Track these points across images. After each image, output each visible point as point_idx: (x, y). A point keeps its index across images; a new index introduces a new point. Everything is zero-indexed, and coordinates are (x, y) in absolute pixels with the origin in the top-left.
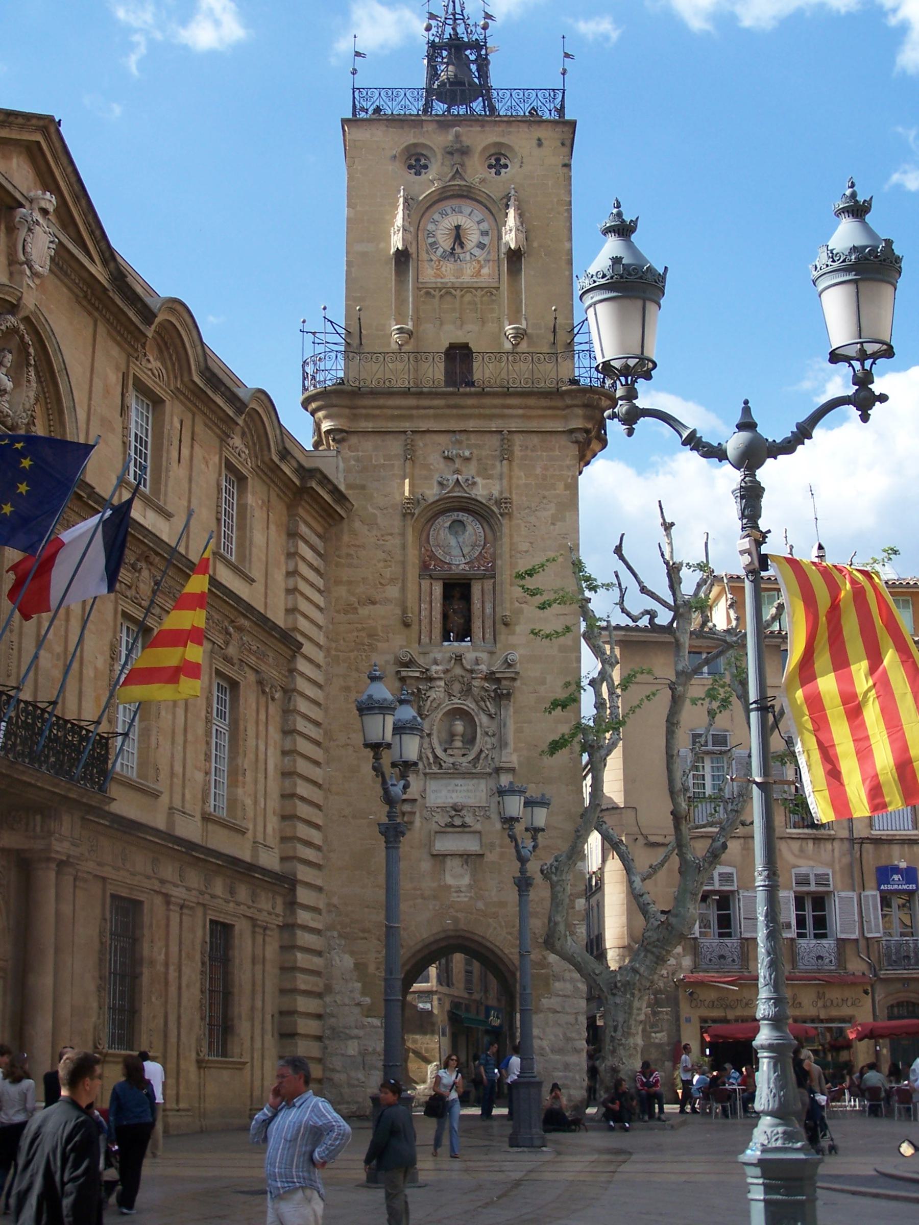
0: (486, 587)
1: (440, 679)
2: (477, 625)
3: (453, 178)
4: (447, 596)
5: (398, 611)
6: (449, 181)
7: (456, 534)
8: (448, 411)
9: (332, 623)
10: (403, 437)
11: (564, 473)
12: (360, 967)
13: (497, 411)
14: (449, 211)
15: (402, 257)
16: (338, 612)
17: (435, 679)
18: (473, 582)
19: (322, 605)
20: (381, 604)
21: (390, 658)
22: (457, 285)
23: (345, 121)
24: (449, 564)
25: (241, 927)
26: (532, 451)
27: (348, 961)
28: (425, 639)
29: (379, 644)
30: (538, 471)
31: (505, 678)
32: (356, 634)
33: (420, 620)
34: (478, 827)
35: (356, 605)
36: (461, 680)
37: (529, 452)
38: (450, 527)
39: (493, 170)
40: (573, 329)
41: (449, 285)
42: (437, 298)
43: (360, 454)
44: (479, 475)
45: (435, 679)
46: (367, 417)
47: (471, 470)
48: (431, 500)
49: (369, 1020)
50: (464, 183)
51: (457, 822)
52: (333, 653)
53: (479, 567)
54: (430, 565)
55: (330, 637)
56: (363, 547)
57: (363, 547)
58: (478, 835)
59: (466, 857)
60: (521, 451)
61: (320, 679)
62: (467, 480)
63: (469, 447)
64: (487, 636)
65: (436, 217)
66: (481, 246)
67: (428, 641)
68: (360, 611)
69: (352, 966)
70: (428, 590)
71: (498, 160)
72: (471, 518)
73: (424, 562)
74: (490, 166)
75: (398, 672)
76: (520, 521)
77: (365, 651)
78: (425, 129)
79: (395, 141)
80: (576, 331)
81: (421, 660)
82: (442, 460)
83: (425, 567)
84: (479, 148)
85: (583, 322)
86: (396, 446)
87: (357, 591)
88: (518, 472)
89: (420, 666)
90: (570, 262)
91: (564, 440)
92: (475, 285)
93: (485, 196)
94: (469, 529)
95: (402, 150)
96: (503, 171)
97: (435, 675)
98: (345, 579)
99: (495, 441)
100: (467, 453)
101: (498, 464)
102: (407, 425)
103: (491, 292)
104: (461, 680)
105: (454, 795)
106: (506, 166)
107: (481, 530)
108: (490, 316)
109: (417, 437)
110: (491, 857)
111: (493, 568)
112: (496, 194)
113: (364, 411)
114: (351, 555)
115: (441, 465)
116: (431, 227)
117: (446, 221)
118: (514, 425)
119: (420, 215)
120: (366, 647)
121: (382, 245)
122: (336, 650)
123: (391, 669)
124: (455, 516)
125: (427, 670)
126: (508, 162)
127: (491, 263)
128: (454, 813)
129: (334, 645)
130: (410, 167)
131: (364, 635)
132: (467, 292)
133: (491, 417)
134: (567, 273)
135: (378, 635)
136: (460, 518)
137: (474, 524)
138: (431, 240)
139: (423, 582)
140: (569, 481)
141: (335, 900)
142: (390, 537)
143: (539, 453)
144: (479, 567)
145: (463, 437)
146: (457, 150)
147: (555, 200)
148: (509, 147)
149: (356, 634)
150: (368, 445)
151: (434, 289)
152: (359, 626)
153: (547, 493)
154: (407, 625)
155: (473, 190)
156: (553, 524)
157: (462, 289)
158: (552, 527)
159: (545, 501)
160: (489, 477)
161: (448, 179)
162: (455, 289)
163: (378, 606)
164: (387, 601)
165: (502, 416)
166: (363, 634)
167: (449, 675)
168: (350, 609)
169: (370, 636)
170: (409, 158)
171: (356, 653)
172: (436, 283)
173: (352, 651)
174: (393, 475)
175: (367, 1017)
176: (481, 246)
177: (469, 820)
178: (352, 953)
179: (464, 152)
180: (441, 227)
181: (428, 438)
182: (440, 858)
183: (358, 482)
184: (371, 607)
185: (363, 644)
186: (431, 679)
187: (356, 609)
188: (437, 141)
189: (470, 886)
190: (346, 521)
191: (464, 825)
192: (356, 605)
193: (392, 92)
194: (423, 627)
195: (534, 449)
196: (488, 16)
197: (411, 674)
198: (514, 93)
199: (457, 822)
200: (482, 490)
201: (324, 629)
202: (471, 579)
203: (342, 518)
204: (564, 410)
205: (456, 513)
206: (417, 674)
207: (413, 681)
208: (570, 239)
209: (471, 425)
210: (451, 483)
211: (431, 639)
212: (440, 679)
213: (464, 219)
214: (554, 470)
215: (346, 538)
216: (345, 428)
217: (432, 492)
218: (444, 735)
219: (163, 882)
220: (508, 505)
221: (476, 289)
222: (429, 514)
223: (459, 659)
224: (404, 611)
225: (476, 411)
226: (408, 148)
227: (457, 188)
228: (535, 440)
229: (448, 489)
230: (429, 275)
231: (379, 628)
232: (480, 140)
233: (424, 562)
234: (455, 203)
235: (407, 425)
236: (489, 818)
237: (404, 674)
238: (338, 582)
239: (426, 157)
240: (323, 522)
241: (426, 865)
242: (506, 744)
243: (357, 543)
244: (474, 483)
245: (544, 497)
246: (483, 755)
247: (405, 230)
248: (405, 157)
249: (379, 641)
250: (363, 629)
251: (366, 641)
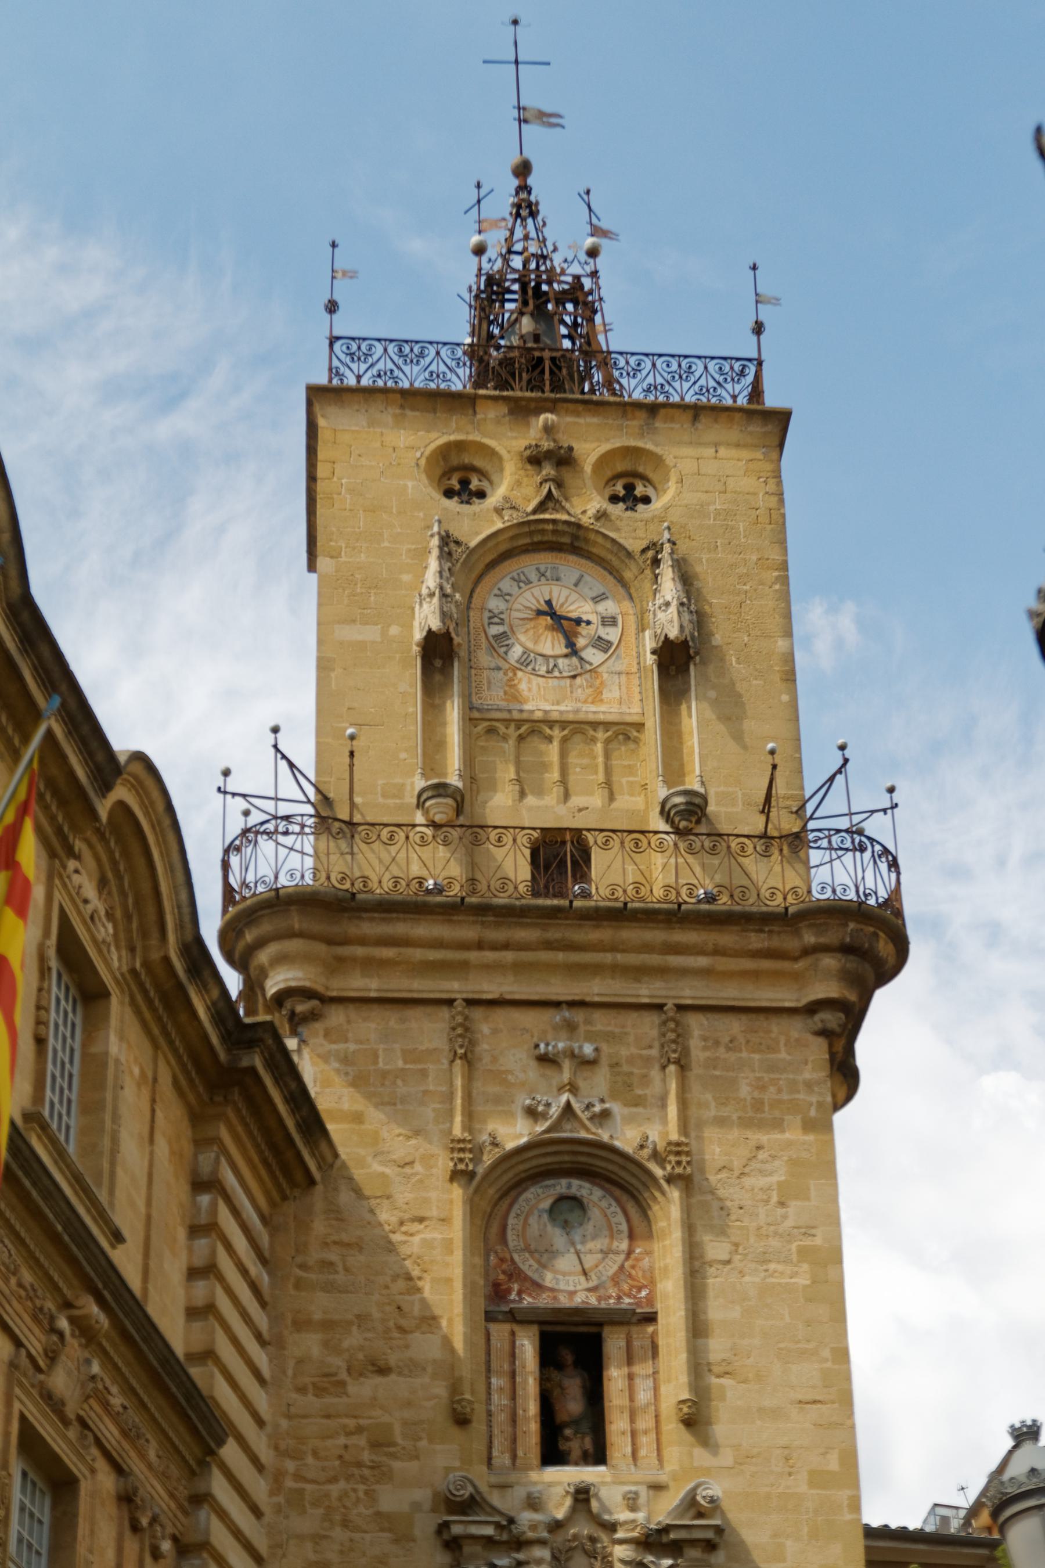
0: (636, 1343)
1: (542, 1542)
2: (617, 1426)
3: (541, 507)
4: (548, 1358)
5: (441, 1390)
6: (535, 512)
7: (566, 1226)
8: (545, 956)
9: (289, 1417)
10: (445, 1013)
11: (801, 1096)
13: (654, 959)
14: (533, 576)
15: (438, 652)
16: (302, 1390)
17: (530, 1543)
18: (607, 1331)
19: (266, 1372)
20: (400, 1374)
21: (422, 1495)
22: (555, 716)
23: (315, 394)
24: (552, 1290)
26: (729, 1049)
28: (501, 1458)
29: (397, 1465)
30: (745, 1091)
31: (693, 1543)
32: (342, 1440)
33: (489, 1414)
35: (343, 1375)
36: (588, 1545)
37: (721, 1052)
38: (552, 1211)
39: (621, 506)
40: (803, 807)
41: (538, 715)
42: (512, 742)
43: (352, 1047)
44: (614, 1095)
45: (530, 1543)
46: (369, 965)
47: (597, 1085)
48: (510, 1145)
50: (565, 517)
52: (289, 1483)
53: (619, 1298)
54: (509, 1291)
55: (283, 1446)
56: (358, 1246)
57: (358, 1246)
60: (705, 1048)
61: (262, 1545)
62: (589, 1106)
63: (590, 1037)
64: (642, 1452)
65: (506, 585)
67: (507, 1460)
68: (351, 1389)
70: (507, 1347)
71: (630, 488)
72: (598, 1193)
73: (496, 1285)
74: (614, 499)
75: (445, 1526)
76: (709, 1197)
77: (364, 1480)
78: (479, 417)
79: (418, 440)
81: (495, 1499)
82: (533, 1063)
83: (497, 1293)
84: (592, 458)
86: (431, 1031)
87: (346, 1344)
88: (697, 1092)
89: (496, 1511)
91: (796, 1028)
92: (591, 717)
93: (609, 545)
94: (595, 1213)
95: (434, 452)
96: (641, 507)
97: (530, 1535)
98: (317, 1316)
99: (648, 1026)
100: (588, 1049)
101: (655, 1073)
102: (456, 985)
103: (624, 732)
104: (588, 1545)
107: (620, 1218)
108: (624, 780)
109: (477, 1013)
111: (650, 1300)
112: (634, 545)
113: (360, 951)
114: (331, 1264)
115: (533, 1072)
116: (495, 604)
117: (528, 594)
118: (690, 992)
119: (474, 575)
120: (367, 1472)
121: (394, 630)
122: (298, 1477)
123: (425, 1525)
124: (563, 1186)
125: (511, 1521)
126: (650, 492)
127: (623, 677)
129: (290, 1466)
130: (449, 493)
131: (361, 1441)
132: (574, 732)
133: (639, 972)
134: (785, 698)
135: (393, 1444)
136: (574, 1191)
137: (604, 1204)
138: (494, 630)
139: (494, 1328)
140: (813, 1113)
142: (416, 1227)
143: (744, 1055)
144: (619, 1298)
145: (579, 1016)
146: (549, 455)
147: (754, 558)
148: (657, 460)
149: (342, 1440)
150: (368, 1027)
151: (507, 722)
152: (351, 1423)
153: (764, 1138)
154: (462, 1421)
155: (581, 533)
156: (782, 1204)
157: (563, 724)
158: (780, 1211)
159: (762, 1155)
160: (638, 1102)
161: (530, 509)
162: (551, 724)
163: (393, 1377)
164: (413, 1368)
165: (662, 972)
166: (361, 1441)
167: (559, 1538)
168: (329, 1384)
169: (375, 1445)
170: (447, 474)
171: (342, 1484)
172: (509, 711)
173: (334, 1480)
174: (425, 1092)
179: (563, 459)
180: (516, 606)
181: (501, 1017)
183: (346, 1106)
184: (379, 1380)
185: (359, 1465)
186: (519, 1544)
187: (342, 1384)
188: (507, 441)
190: (319, 1188)
192: (343, 1375)
193: (409, 349)
194: (496, 1431)
195: (732, 1045)
196: (596, 231)
197: (474, 1530)
198: (660, 362)
201: (269, 1429)
202: (601, 1325)
203: (312, 1182)
204: (796, 959)
205: (564, 1182)
206: (489, 1531)
207: (478, 1549)
209: (596, 989)
210: (555, 1111)
211: (514, 1457)
212: (542, 1542)
213: (565, 592)
214: (780, 1091)
215: (319, 1226)
216: (320, 989)
217: (515, 1133)
220: (684, 1159)
221: (595, 725)
222: (505, 1178)
223: (582, 1495)
224: (455, 1388)
225: (608, 958)
226: (446, 451)
227: (550, 527)
228: (735, 1025)
229: (547, 1124)
230: (493, 697)
231: (397, 1429)
232: (592, 442)
233: (496, 1285)
234: (545, 560)
235: (455, 987)
237: (457, 1530)
238: (301, 1324)
239: (483, 474)
240: (270, 1184)
243: (344, 1237)
244: (605, 1114)
245: (758, 1148)
247: (444, 596)
248: (439, 472)
249: (394, 1456)
250: (359, 1430)
251: (366, 1456)
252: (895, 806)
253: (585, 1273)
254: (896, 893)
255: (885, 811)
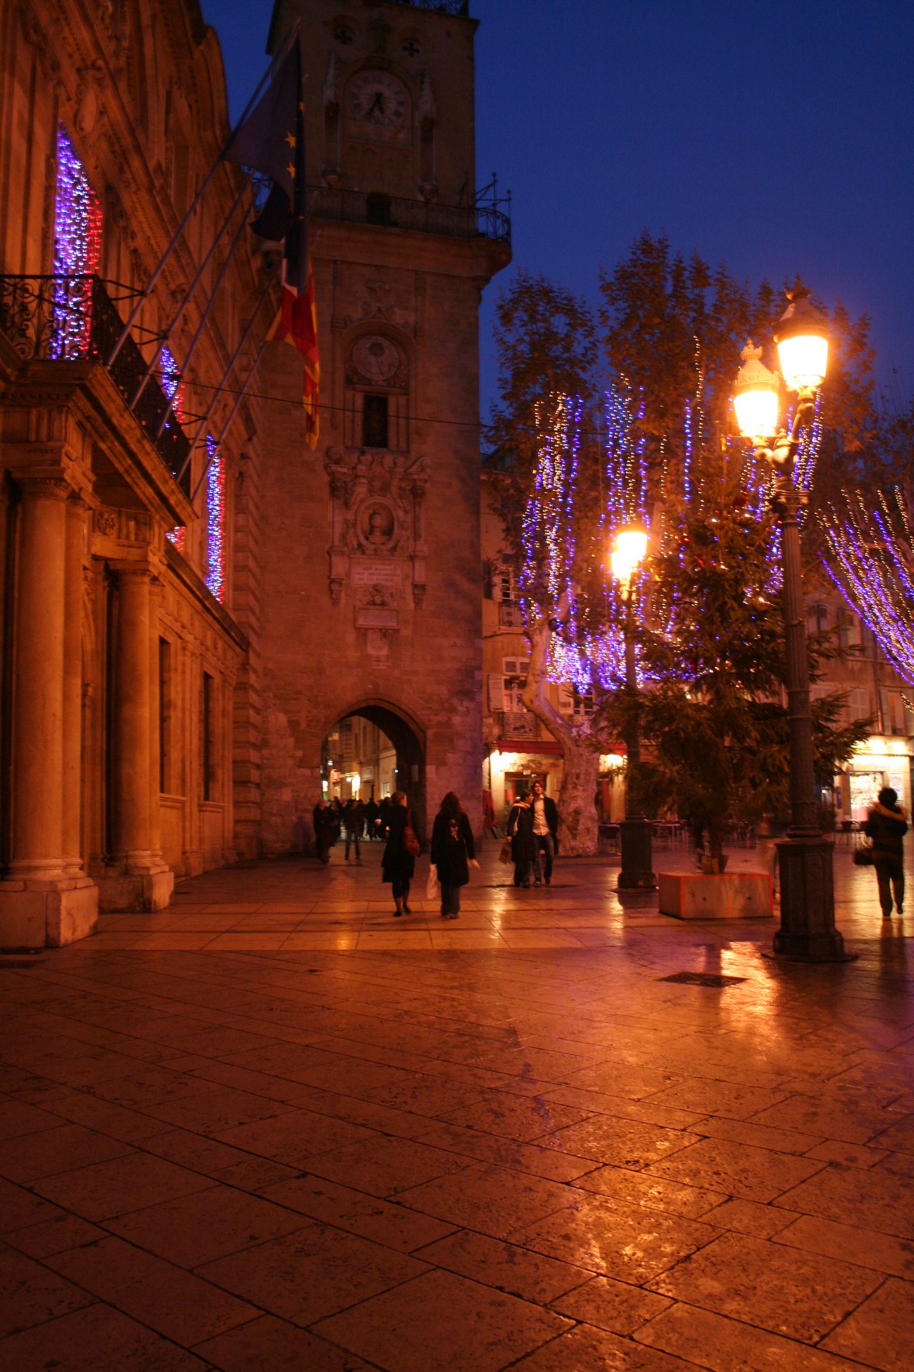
7: (375, 355)
12: (293, 724)
17: (360, 476)
24: (369, 379)
25: (217, 680)
27: (283, 718)
34: (394, 605)
49: (301, 770)
51: (378, 599)
58: (395, 613)
59: (385, 633)
66: (397, 114)
67: (350, 443)
69: (286, 723)
74: (405, 49)
80: (478, 196)
85: (489, 187)
90: (472, 139)
100: (387, 287)
105: (375, 577)
106: (418, 51)
110: (406, 632)
128: (375, 593)
141: (270, 665)
175: (300, 767)
176: (397, 114)
177: (387, 599)
178: (286, 712)
182: (362, 633)
189: (388, 657)
191: (383, 604)
199: (378, 599)
200: (400, 317)
205: (374, 337)
208: (473, 119)
212: (364, 477)
218: (367, 526)
219: (184, 627)
236: (404, 598)
241: (350, 638)
242: (420, 537)
246: (400, 544)
252: (510, 199)
253: (382, 374)
254: (509, 234)
255: (506, 200)
